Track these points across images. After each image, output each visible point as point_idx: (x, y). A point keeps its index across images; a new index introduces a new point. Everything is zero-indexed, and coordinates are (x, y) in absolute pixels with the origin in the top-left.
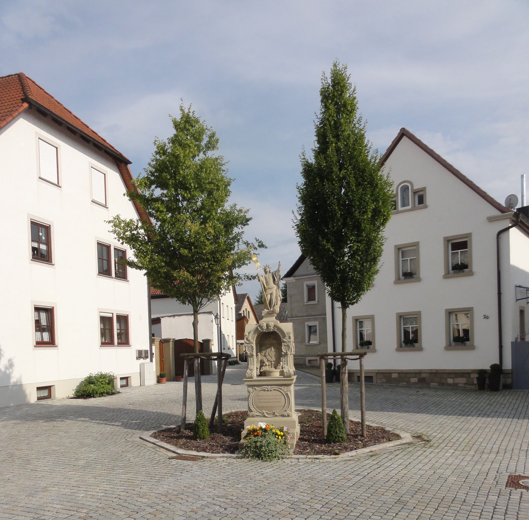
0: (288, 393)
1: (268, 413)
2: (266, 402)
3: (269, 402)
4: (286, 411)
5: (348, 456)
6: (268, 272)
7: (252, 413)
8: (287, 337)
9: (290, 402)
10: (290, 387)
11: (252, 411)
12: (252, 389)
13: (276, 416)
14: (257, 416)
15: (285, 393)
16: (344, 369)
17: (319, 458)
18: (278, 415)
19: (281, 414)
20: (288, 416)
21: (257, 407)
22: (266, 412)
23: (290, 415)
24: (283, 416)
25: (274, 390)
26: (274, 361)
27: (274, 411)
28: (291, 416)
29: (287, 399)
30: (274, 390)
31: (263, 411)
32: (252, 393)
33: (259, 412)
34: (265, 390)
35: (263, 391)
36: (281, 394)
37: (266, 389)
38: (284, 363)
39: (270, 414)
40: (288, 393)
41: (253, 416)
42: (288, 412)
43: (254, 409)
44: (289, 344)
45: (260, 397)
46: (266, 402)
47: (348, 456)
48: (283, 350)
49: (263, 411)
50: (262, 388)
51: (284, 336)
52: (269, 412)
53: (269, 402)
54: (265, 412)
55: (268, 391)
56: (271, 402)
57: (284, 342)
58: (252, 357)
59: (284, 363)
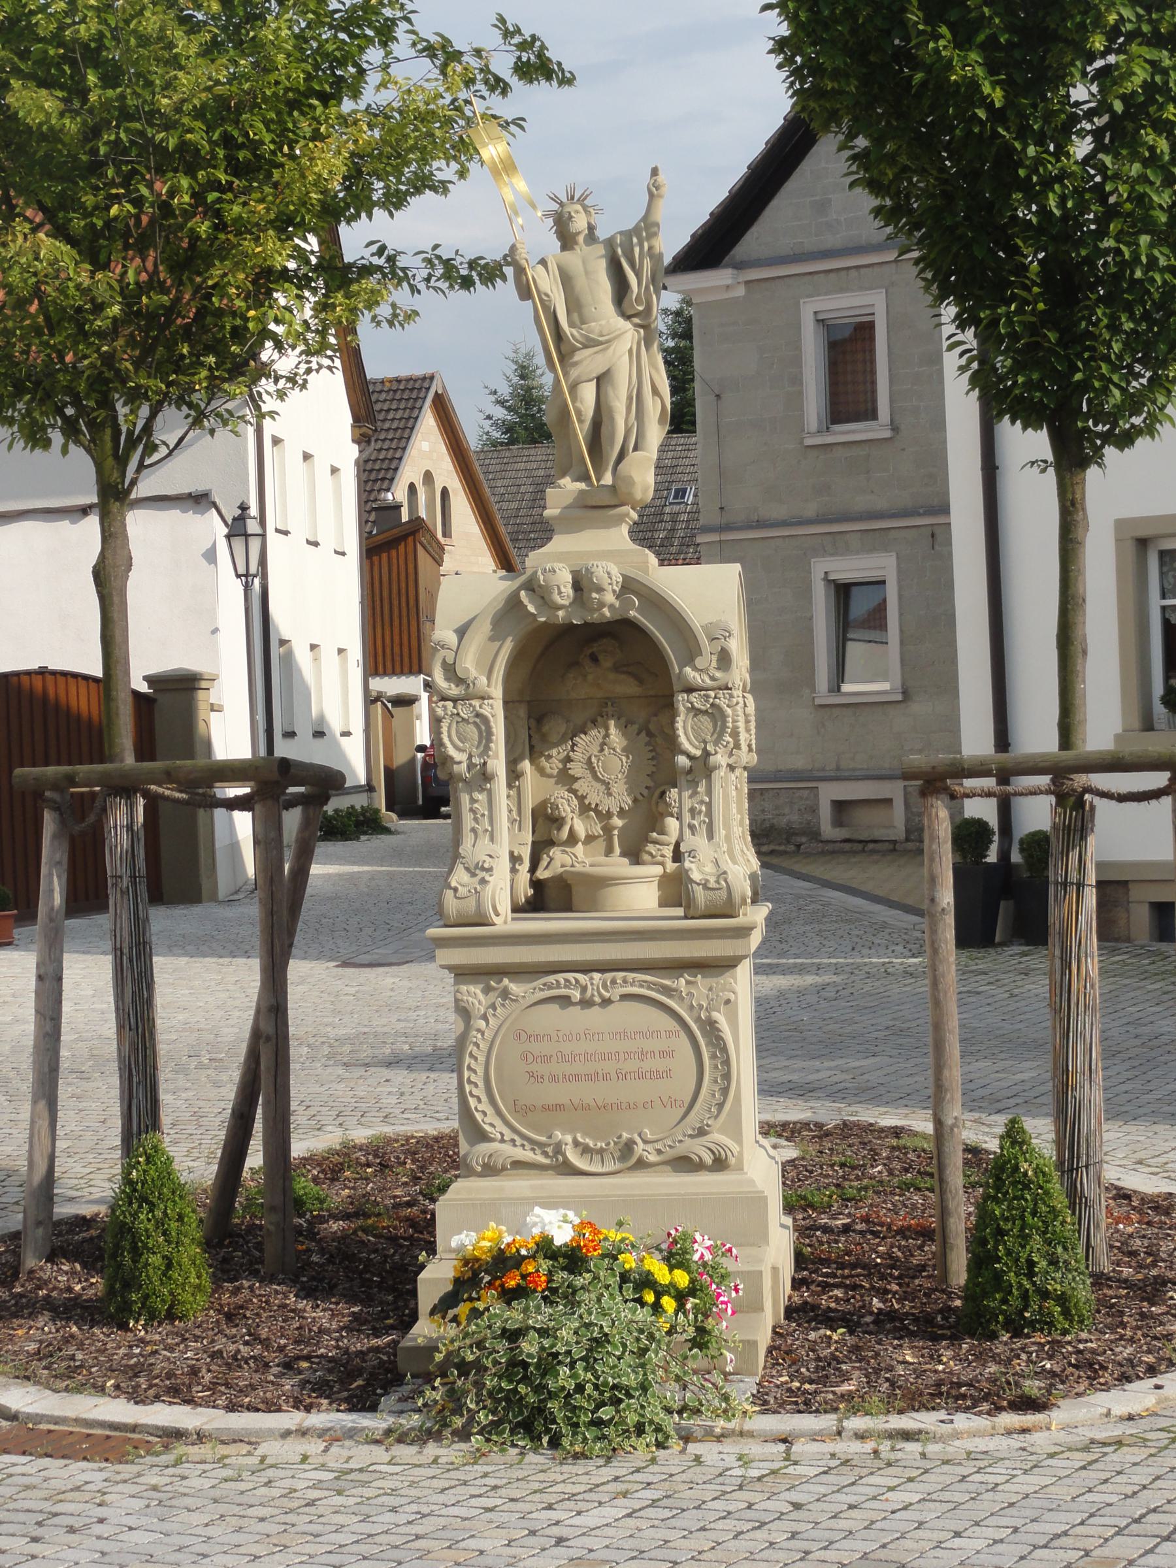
0: (720, 1018)
1: (586, 1150)
2: (577, 1077)
3: (593, 1077)
4: (702, 1132)
5: (1108, 1414)
6: (581, 239)
7: (484, 1148)
8: (707, 659)
9: (727, 1076)
10: (725, 979)
11: (484, 1137)
12: (487, 990)
13: (641, 1164)
14: (518, 1164)
15: (698, 1020)
16: (1074, 856)
17: (920, 1432)
18: (653, 1158)
19: (670, 1154)
20: (720, 1164)
21: (516, 1109)
22: (576, 1143)
23: (732, 1161)
24: (685, 1164)
25: (625, 997)
26: (622, 813)
27: (625, 1135)
28: (740, 1168)
29: (713, 1057)
30: (625, 997)
31: (558, 1135)
32: (485, 1018)
34: (565, 1001)
35: (554, 1007)
36: (672, 1024)
37: (576, 995)
38: (692, 827)
39: (601, 1152)
40: (716, 1015)
41: (490, 1170)
42: (716, 1137)
43: (498, 1122)
44: (722, 703)
45: (536, 1048)
46: (577, 1077)
47: (1108, 1414)
48: (682, 739)
49: (558, 1135)
50: (550, 987)
51: (691, 652)
52: (595, 1139)
53: (593, 1077)
54: (569, 1138)
55: (586, 1003)
56: (606, 1077)
57: (690, 690)
58: (482, 790)
59: (692, 827)
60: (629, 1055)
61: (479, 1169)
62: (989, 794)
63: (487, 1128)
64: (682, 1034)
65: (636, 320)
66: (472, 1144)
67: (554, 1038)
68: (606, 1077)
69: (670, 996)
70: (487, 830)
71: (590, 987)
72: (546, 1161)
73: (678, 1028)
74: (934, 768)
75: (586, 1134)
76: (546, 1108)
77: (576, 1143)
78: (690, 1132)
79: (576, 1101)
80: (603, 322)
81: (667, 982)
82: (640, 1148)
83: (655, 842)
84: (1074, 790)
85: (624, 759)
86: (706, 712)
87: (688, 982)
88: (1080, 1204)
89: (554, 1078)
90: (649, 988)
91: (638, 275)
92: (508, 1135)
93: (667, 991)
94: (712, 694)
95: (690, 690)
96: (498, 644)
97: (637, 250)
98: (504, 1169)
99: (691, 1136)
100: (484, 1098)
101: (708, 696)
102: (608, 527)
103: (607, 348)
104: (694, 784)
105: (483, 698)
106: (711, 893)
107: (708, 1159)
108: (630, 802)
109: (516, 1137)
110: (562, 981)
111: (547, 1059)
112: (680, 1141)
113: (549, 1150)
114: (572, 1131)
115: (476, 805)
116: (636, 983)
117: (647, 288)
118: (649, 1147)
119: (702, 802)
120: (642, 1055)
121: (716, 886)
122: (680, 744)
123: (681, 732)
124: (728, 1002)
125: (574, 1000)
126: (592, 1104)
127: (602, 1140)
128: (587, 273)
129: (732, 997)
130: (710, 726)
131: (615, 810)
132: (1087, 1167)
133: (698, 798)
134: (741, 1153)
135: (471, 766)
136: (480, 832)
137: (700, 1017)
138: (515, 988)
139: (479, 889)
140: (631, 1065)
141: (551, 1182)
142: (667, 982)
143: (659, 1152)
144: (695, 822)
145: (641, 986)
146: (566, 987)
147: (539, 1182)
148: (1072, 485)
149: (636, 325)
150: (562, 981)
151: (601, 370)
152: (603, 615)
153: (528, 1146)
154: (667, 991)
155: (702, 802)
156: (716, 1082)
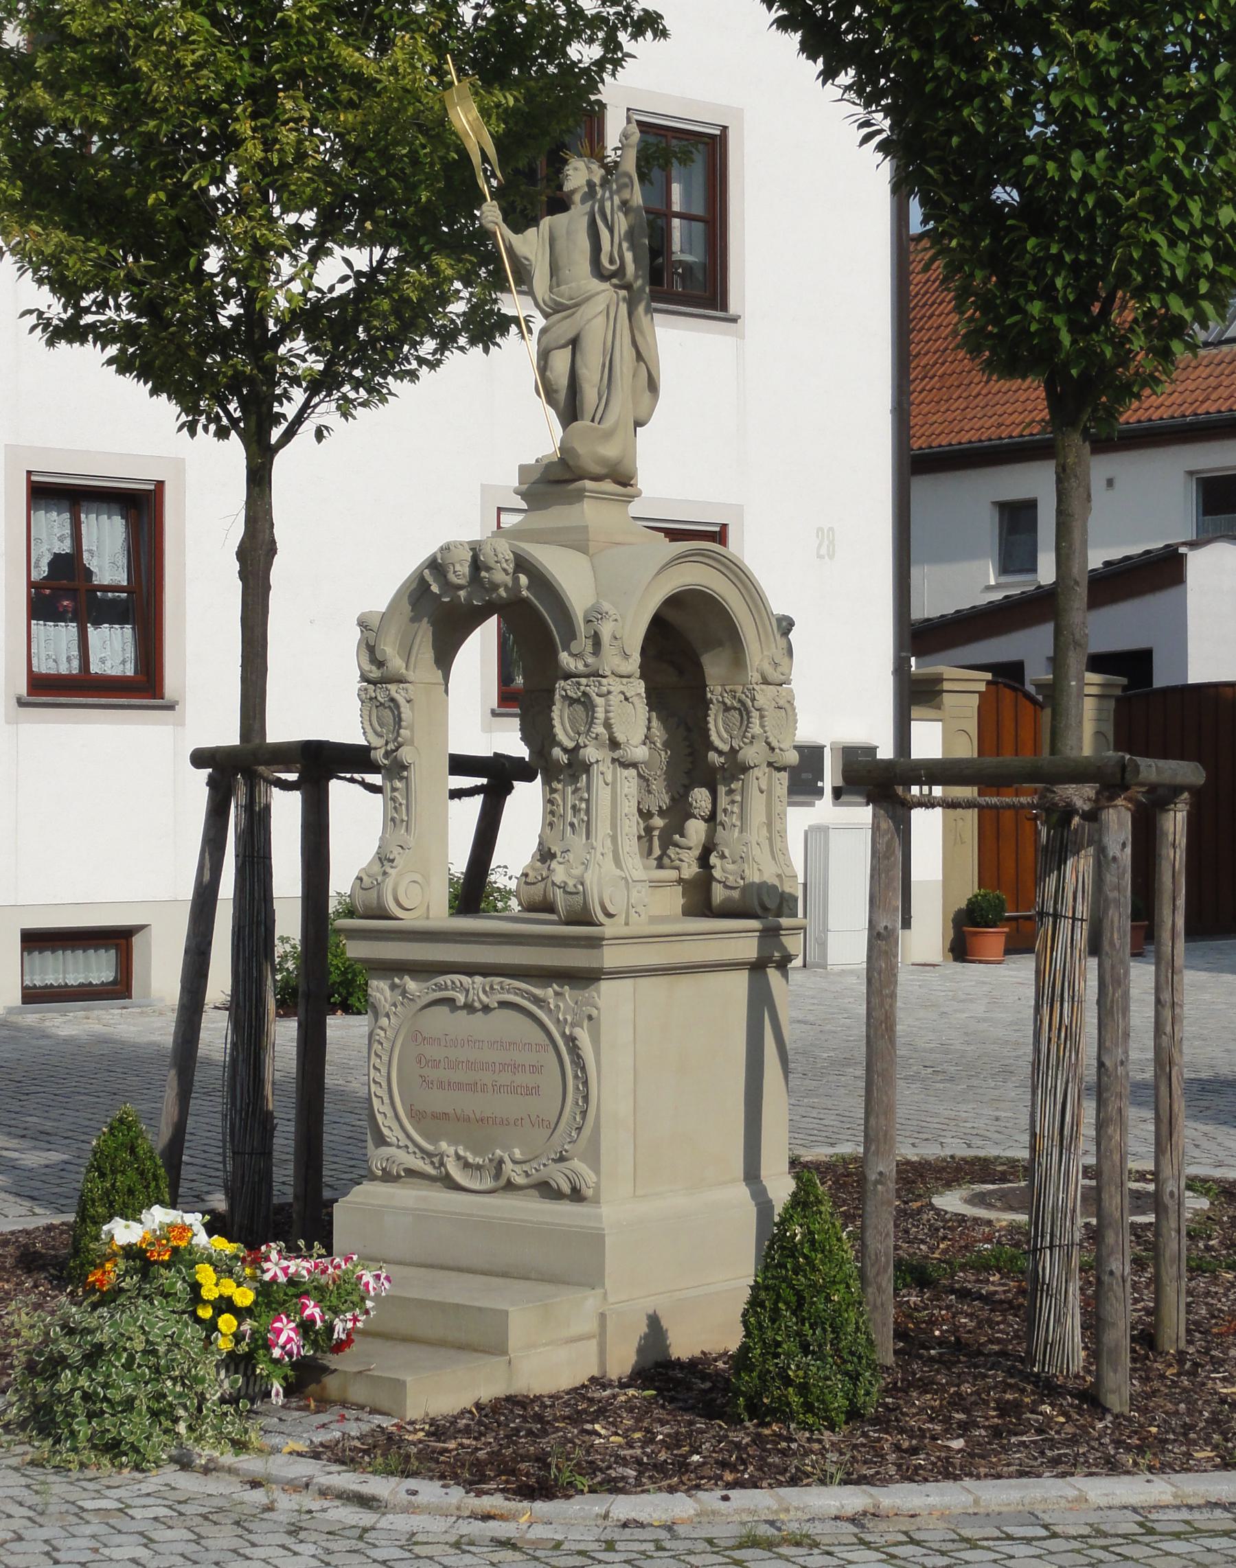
0: (583, 1036)
1: (467, 1165)
2: (459, 1086)
3: (472, 1087)
4: (562, 1159)
5: (606, 1516)
6: (577, 198)
7: (385, 1151)
8: (582, 643)
9: (586, 1098)
10: (590, 993)
11: (381, 1141)
12: (393, 987)
13: (510, 1186)
14: (411, 1173)
15: (563, 1035)
16: (1052, 881)
17: (374, 1499)
18: (520, 1180)
19: (536, 1177)
20: (576, 1195)
21: (411, 1117)
22: (458, 1157)
23: (589, 1193)
24: (546, 1190)
25: (503, 1004)
26: (661, 813)
27: (498, 1152)
28: (596, 1201)
29: (576, 1077)
30: (503, 1004)
31: (444, 1145)
32: (387, 1015)
33: (422, 1150)
34: (450, 1002)
35: (445, 1009)
36: (541, 1037)
37: (461, 999)
38: (572, 825)
39: (479, 1167)
40: (578, 1032)
41: (388, 1177)
42: (576, 1164)
43: (395, 1126)
44: (592, 691)
45: (432, 1052)
46: (459, 1086)
47: (606, 1516)
48: (558, 730)
49: (444, 1145)
50: (440, 988)
51: (570, 633)
52: (475, 1154)
53: (472, 1087)
54: (451, 1151)
55: (469, 1008)
56: (484, 1088)
57: (568, 676)
58: (401, 778)
59: (572, 825)
60: (504, 1066)
61: (380, 1173)
62: (969, 805)
63: (386, 1131)
64: (551, 1048)
65: (615, 281)
66: (377, 1147)
67: (443, 1043)
68: (484, 1088)
69: (540, 1007)
70: (402, 821)
71: (471, 991)
72: (433, 1172)
73: (547, 1042)
74: (869, 771)
75: (466, 1148)
76: (435, 1116)
77: (458, 1157)
78: (553, 1156)
79: (459, 1112)
80: (573, 285)
81: (538, 992)
82: (508, 1167)
83: (677, 845)
84: (1056, 804)
85: (663, 753)
86: (577, 701)
87: (557, 994)
88: (1042, 1290)
89: (441, 1085)
90: (523, 997)
91: (611, 231)
92: (404, 1141)
93: (537, 1001)
94: (583, 681)
95: (568, 676)
96: (416, 625)
97: (608, 204)
98: (399, 1177)
99: (553, 1160)
100: (387, 1100)
101: (579, 684)
102: (571, 504)
103: (573, 313)
104: (574, 778)
105: (401, 682)
106: (569, 897)
107: (566, 1188)
108: (667, 801)
109: (409, 1144)
110: (449, 983)
111: (436, 1064)
112: (545, 1165)
113: (436, 1160)
114: (453, 1142)
115: (396, 794)
116: (510, 990)
117: (620, 245)
118: (518, 1168)
119: (581, 799)
120: (516, 1068)
121: (574, 890)
122: (554, 736)
123: (556, 722)
124: (590, 1018)
125: (458, 1004)
126: (472, 1116)
127: (481, 1156)
128: (568, 233)
129: (595, 1013)
130: (584, 717)
131: (654, 810)
132: (1051, 1247)
133: (579, 793)
134: (598, 1184)
135: (387, 754)
136: (398, 822)
137: (564, 1033)
138: (411, 985)
139: (380, 879)
140: (505, 1078)
141: (437, 1194)
142: (538, 992)
143: (527, 1174)
144: (575, 821)
145: (516, 994)
146: (453, 989)
147: (424, 1193)
148: (1064, 448)
149: (615, 286)
150: (449, 983)
151: (571, 335)
152: (499, 595)
153: (419, 1155)
154: (537, 1001)
155: (581, 799)
156: (577, 1103)
